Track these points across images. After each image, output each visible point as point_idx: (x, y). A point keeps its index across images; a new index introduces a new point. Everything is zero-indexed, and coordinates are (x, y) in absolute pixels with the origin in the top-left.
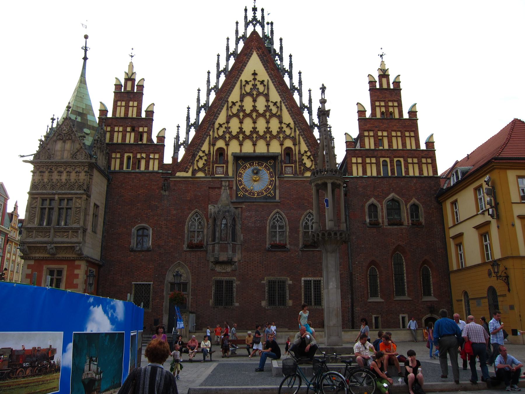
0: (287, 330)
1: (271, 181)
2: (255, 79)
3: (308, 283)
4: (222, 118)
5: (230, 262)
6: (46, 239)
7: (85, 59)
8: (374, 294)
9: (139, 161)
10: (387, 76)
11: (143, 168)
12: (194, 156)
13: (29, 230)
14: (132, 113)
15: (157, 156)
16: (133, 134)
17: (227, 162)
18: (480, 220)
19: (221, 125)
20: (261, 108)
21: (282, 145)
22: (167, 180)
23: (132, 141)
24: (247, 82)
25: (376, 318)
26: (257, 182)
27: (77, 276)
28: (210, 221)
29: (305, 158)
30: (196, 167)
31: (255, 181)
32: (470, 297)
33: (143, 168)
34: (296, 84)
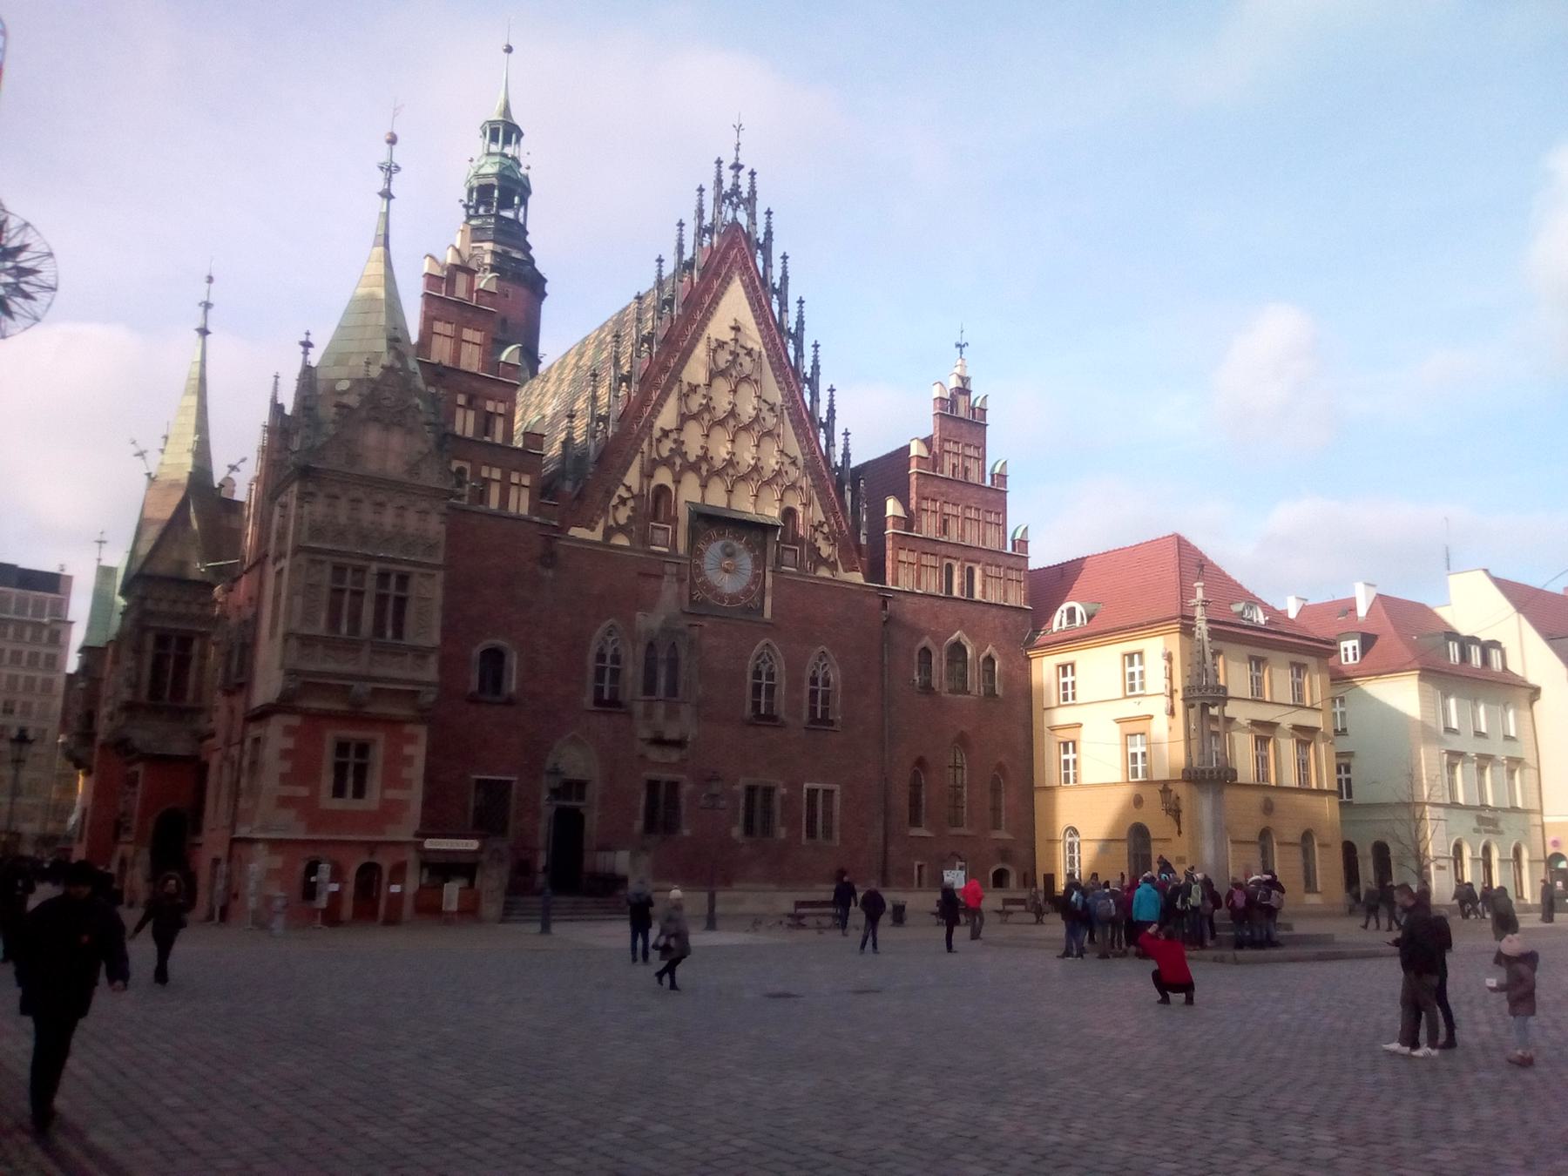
0: (772, 886)
1: (756, 576)
2: (736, 340)
3: (812, 793)
4: (667, 417)
5: (679, 744)
6: (347, 668)
7: (387, 195)
8: (915, 821)
9: (487, 482)
10: (967, 392)
11: (494, 503)
12: (609, 494)
13: (307, 641)
14: (471, 359)
15: (526, 481)
16: (471, 415)
17: (675, 520)
18: (1131, 708)
19: (666, 433)
20: (747, 410)
21: (781, 500)
22: (549, 540)
23: (470, 433)
24: (721, 344)
25: (920, 867)
26: (728, 573)
27: (409, 761)
28: (641, 649)
29: (819, 536)
30: (611, 522)
31: (727, 571)
32: (1083, 836)
33: (494, 503)
34: (808, 370)
